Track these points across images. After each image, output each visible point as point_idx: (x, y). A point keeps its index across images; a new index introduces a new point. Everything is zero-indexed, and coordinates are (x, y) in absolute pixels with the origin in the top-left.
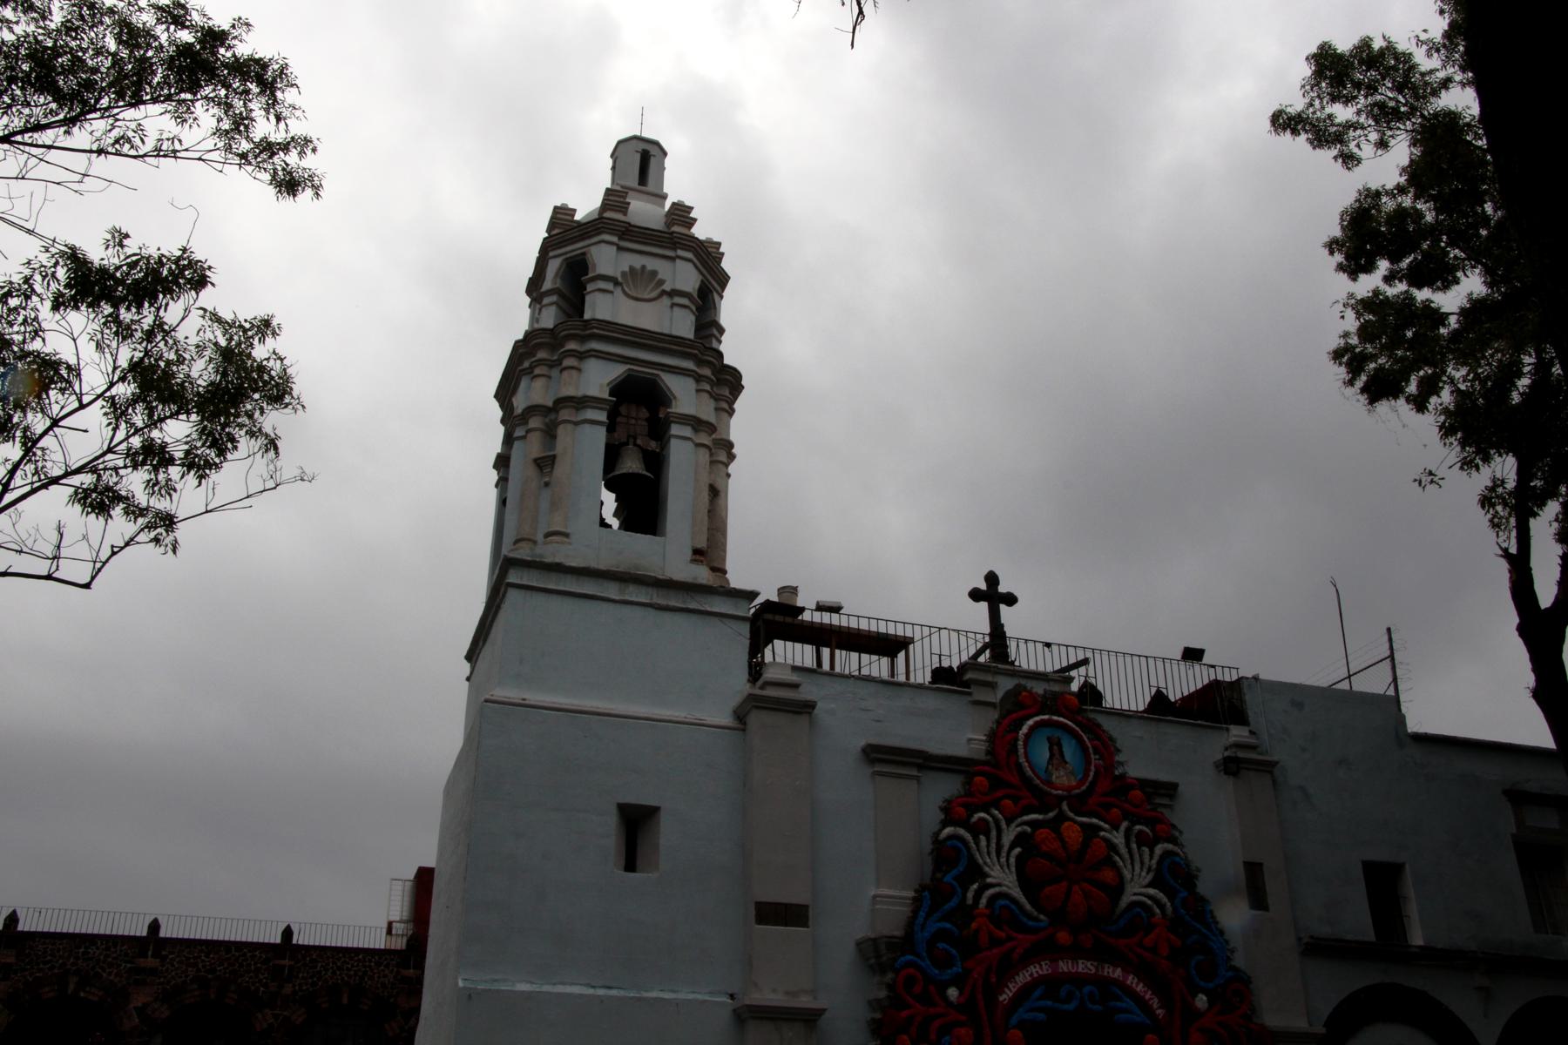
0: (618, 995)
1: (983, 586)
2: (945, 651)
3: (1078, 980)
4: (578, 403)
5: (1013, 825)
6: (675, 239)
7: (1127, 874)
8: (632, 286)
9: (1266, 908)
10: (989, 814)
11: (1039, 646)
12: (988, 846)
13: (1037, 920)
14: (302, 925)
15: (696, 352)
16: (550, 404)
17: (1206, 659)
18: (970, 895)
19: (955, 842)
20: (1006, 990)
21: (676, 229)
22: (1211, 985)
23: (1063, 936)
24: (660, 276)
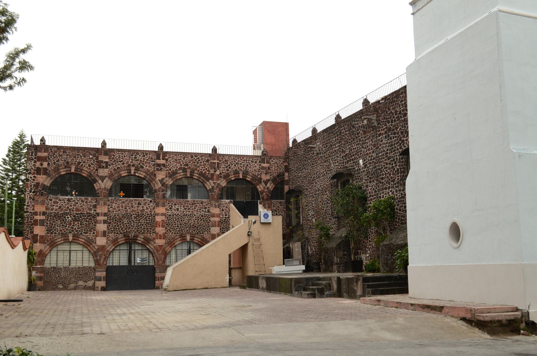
14: (220, 146)
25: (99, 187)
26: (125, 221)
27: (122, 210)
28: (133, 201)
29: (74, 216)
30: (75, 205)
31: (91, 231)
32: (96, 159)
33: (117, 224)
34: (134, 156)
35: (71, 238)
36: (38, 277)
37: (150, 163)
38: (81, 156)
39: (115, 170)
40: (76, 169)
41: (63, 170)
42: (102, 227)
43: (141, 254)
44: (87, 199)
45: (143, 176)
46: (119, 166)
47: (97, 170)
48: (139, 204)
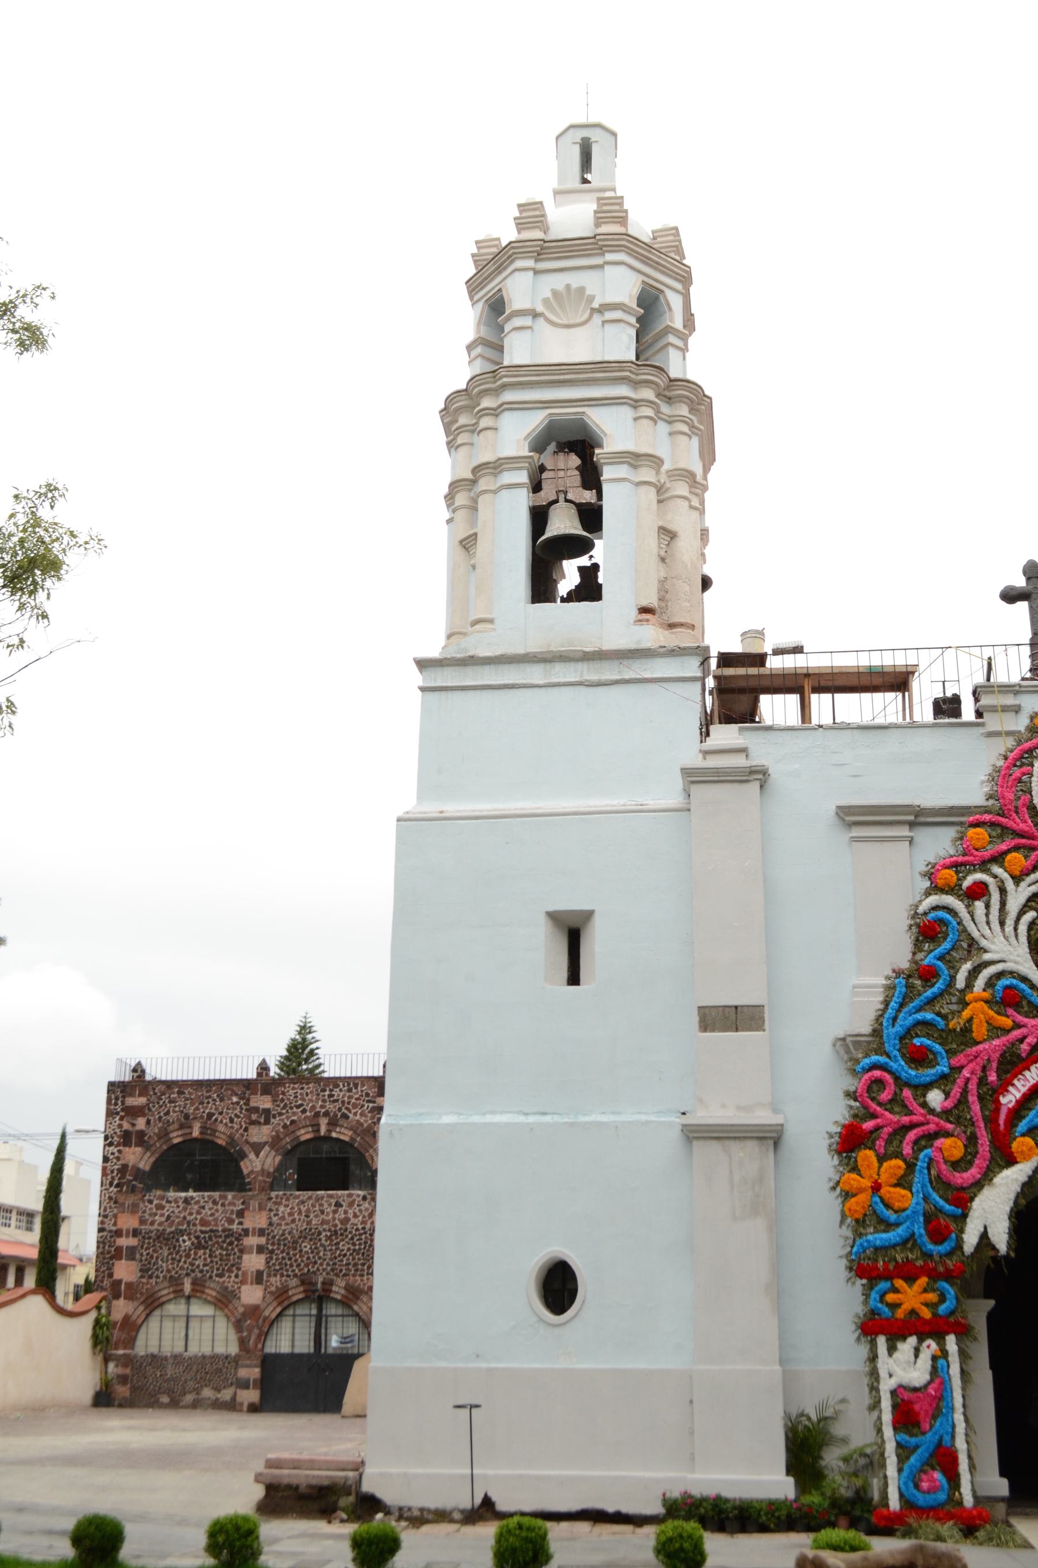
0: (551, 1121)
2: (951, 675)
4: (494, 468)
5: (1023, 884)
6: (600, 243)
8: (560, 312)
10: (987, 871)
12: (987, 915)
15: (627, 374)
16: (470, 476)
19: (941, 914)
20: (1011, 1088)
21: (605, 229)
24: (588, 292)
25: (250, 1169)
26: (305, 1247)
27: (299, 1220)
28: (323, 1198)
29: (197, 1238)
30: (198, 1213)
31: (230, 1271)
32: (245, 1104)
33: (288, 1254)
34: (327, 1093)
35: (187, 1287)
36: (119, 1376)
37: (363, 1106)
38: (214, 1100)
39: (285, 1126)
40: (204, 1129)
41: (175, 1134)
42: (253, 1262)
43: (340, 1325)
44: (225, 1197)
45: (347, 1139)
46: (295, 1118)
47: (246, 1129)
48: (338, 1205)
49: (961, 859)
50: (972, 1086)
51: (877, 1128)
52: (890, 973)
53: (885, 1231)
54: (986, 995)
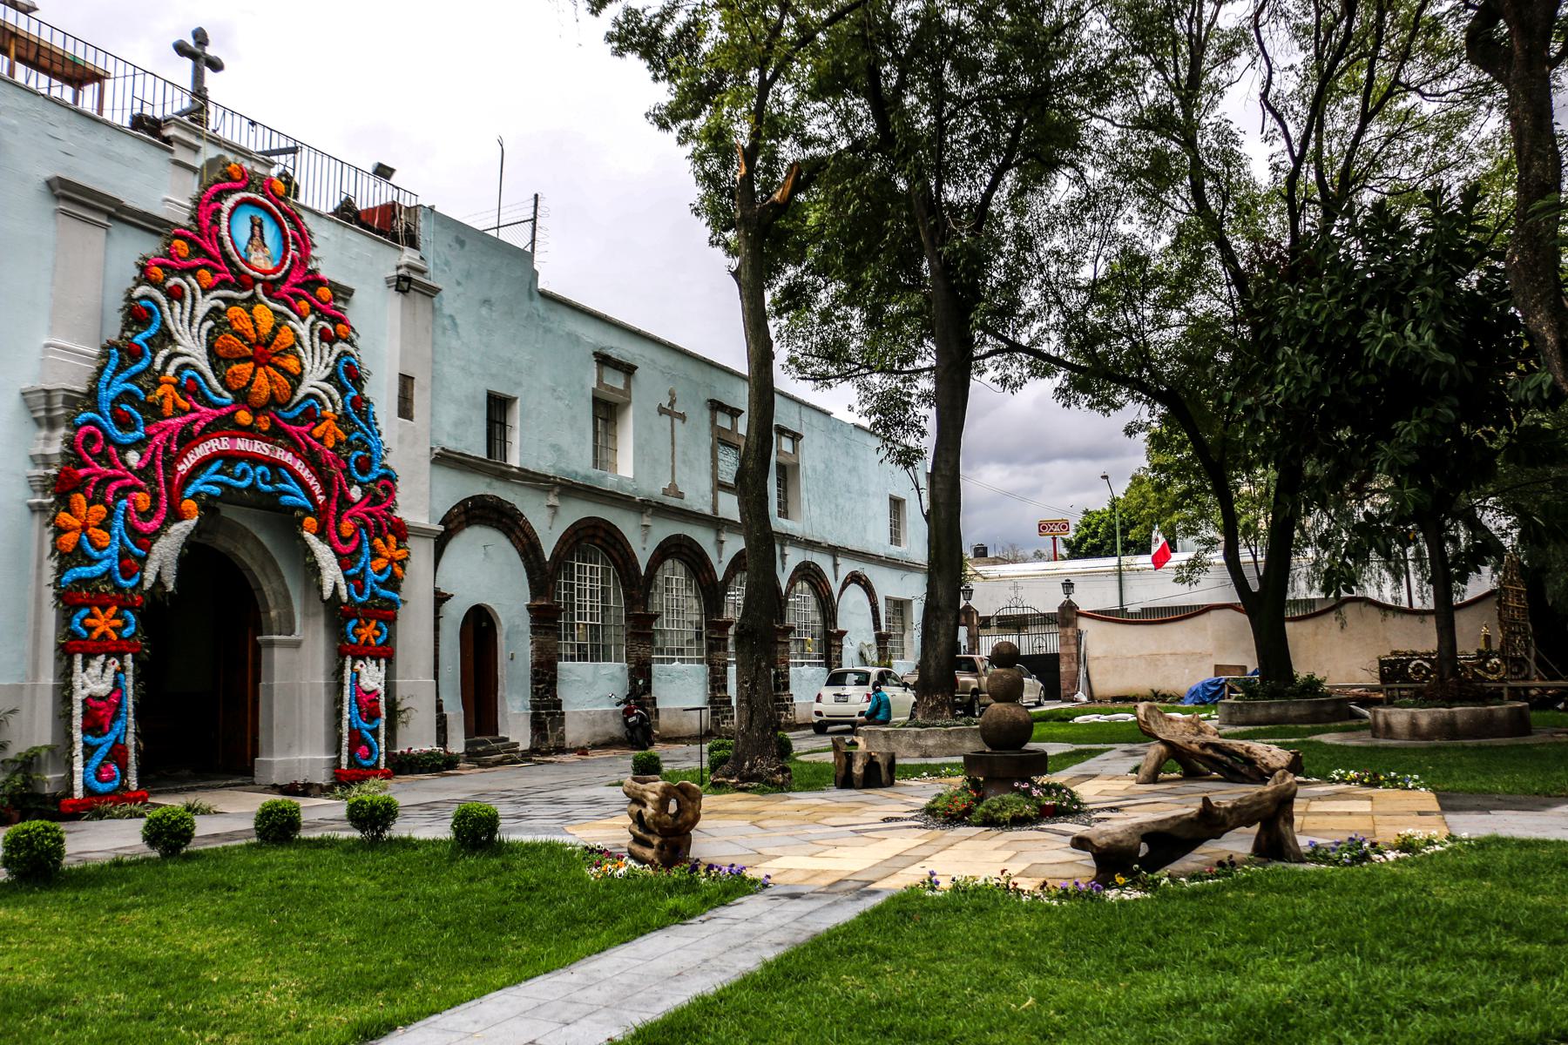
1: (191, 42)
2: (148, 98)
3: (255, 460)
5: (208, 297)
7: (308, 367)
9: (411, 418)
10: (184, 278)
11: (246, 122)
12: (182, 313)
13: (220, 395)
17: (391, 181)
18: (159, 360)
22: (366, 479)
23: (244, 417)
49: (168, 261)
50: (160, 453)
51: (89, 475)
52: (105, 342)
53: (89, 565)
54: (174, 380)
